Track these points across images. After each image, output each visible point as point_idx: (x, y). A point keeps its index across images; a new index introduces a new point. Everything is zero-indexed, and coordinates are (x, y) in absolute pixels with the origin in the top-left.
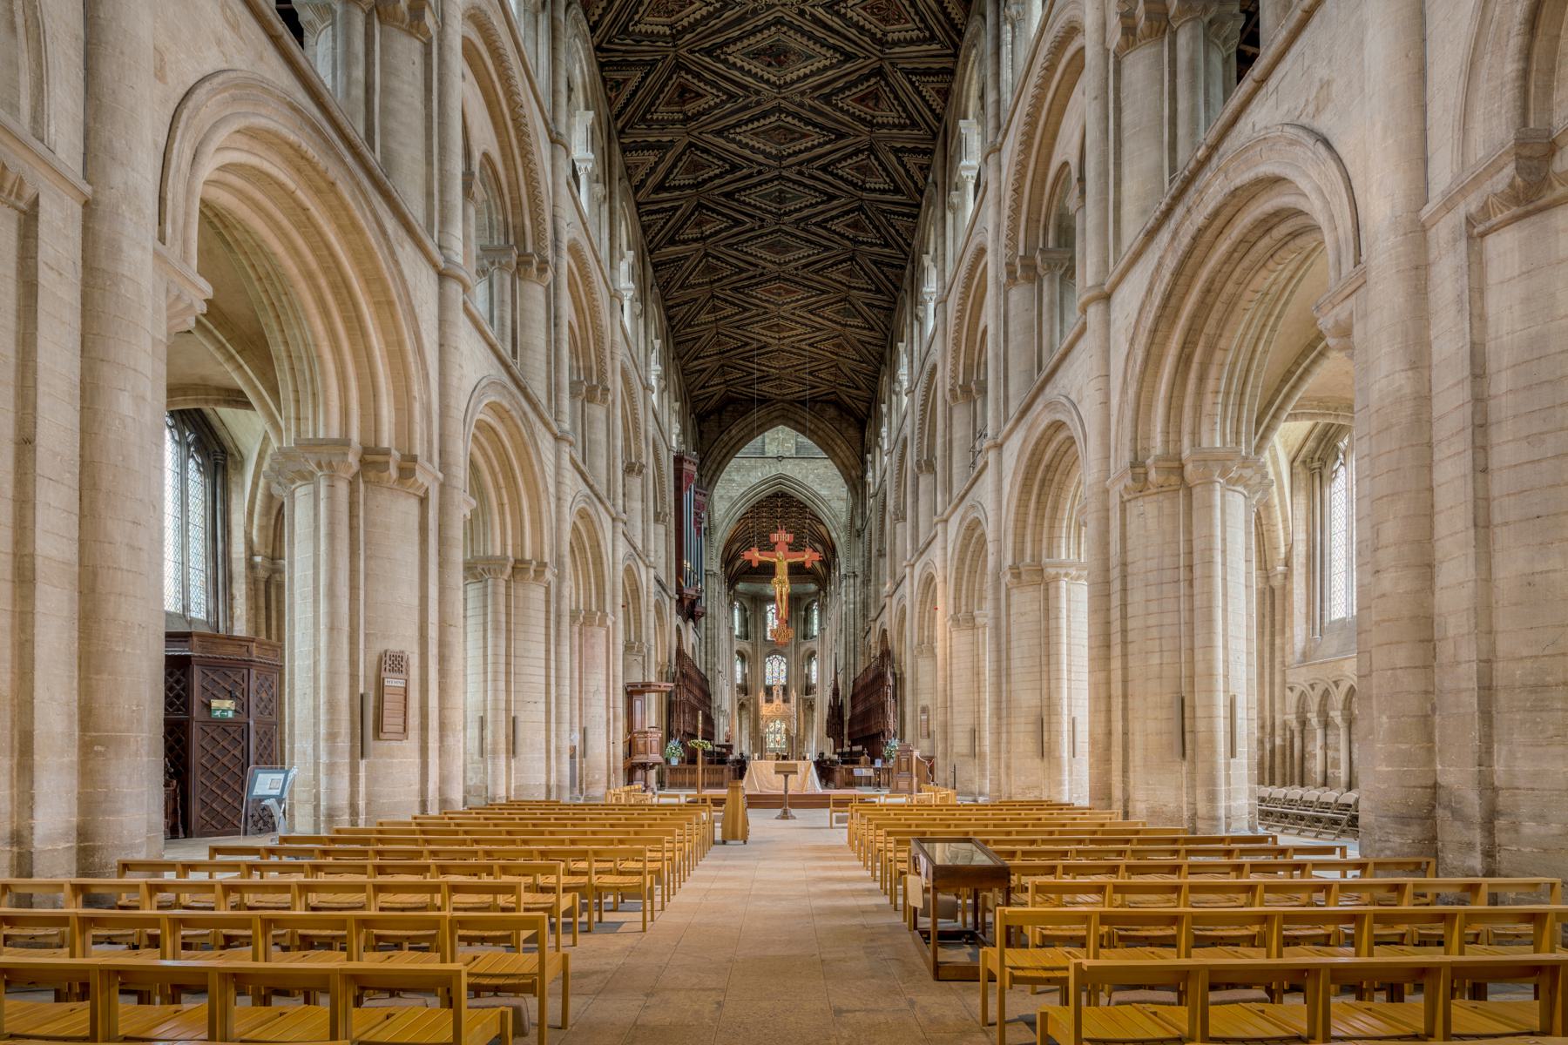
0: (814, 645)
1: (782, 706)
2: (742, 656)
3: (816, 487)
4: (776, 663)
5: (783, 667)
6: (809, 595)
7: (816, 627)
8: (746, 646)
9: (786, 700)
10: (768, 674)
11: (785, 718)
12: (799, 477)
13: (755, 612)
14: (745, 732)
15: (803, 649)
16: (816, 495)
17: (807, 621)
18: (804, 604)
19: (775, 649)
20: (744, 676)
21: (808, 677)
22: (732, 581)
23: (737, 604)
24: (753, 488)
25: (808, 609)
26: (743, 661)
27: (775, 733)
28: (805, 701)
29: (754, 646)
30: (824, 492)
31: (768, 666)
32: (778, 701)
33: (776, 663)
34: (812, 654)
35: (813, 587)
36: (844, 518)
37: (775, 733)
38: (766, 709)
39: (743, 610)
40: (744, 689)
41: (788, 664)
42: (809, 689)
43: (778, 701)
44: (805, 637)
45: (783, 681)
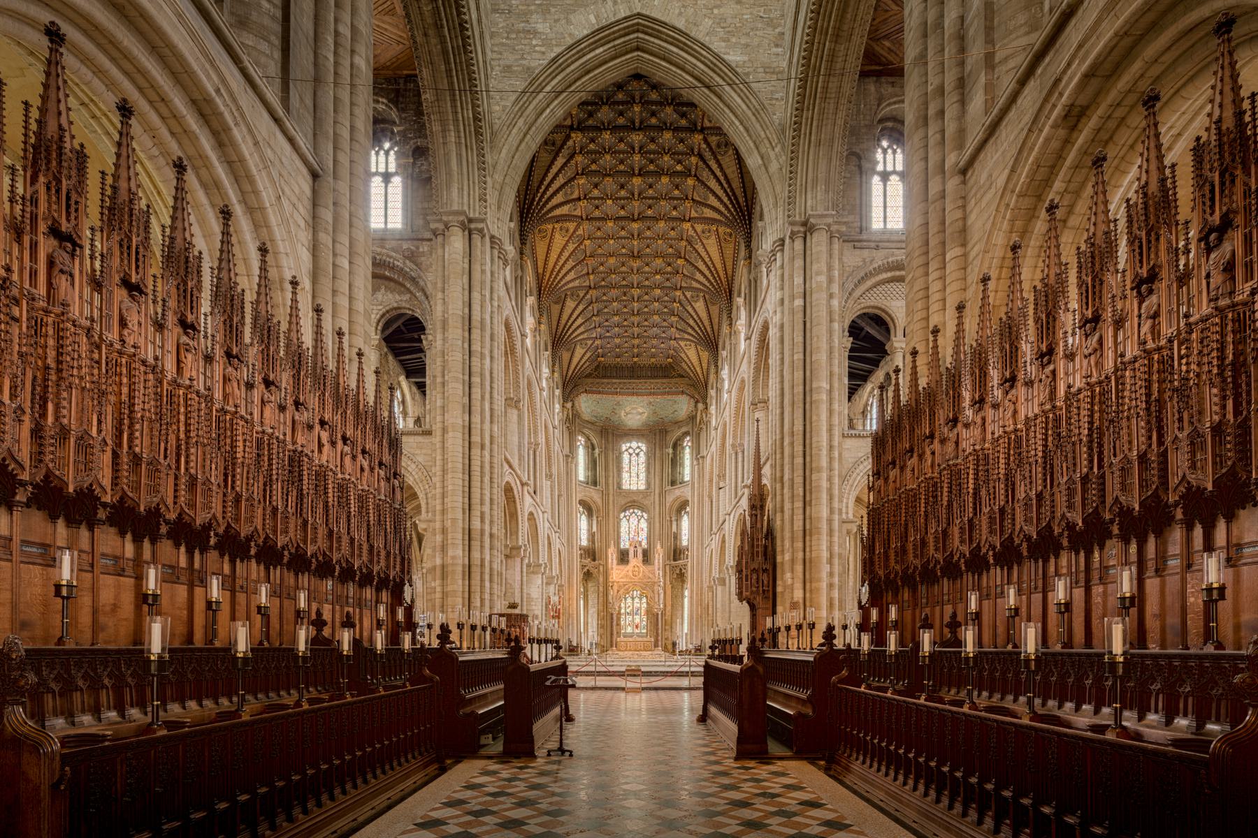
1: (642, 568)
3: (717, 46)
4: (634, 520)
5: (644, 525)
6: (677, 423)
7: (687, 471)
9: (647, 557)
10: (624, 535)
11: (647, 587)
12: (681, 24)
13: (605, 451)
14: (593, 611)
15: (670, 499)
16: (718, 63)
17: (675, 462)
18: (671, 439)
19: (633, 502)
22: (571, 386)
23: (581, 440)
24: (577, 48)
27: (632, 614)
29: (605, 495)
30: (733, 57)
31: (624, 523)
32: (635, 561)
33: (634, 520)
35: (682, 406)
37: (632, 614)
38: (618, 573)
39: (591, 447)
41: (649, 522)
43: (635, 561)
44: (673, 483)
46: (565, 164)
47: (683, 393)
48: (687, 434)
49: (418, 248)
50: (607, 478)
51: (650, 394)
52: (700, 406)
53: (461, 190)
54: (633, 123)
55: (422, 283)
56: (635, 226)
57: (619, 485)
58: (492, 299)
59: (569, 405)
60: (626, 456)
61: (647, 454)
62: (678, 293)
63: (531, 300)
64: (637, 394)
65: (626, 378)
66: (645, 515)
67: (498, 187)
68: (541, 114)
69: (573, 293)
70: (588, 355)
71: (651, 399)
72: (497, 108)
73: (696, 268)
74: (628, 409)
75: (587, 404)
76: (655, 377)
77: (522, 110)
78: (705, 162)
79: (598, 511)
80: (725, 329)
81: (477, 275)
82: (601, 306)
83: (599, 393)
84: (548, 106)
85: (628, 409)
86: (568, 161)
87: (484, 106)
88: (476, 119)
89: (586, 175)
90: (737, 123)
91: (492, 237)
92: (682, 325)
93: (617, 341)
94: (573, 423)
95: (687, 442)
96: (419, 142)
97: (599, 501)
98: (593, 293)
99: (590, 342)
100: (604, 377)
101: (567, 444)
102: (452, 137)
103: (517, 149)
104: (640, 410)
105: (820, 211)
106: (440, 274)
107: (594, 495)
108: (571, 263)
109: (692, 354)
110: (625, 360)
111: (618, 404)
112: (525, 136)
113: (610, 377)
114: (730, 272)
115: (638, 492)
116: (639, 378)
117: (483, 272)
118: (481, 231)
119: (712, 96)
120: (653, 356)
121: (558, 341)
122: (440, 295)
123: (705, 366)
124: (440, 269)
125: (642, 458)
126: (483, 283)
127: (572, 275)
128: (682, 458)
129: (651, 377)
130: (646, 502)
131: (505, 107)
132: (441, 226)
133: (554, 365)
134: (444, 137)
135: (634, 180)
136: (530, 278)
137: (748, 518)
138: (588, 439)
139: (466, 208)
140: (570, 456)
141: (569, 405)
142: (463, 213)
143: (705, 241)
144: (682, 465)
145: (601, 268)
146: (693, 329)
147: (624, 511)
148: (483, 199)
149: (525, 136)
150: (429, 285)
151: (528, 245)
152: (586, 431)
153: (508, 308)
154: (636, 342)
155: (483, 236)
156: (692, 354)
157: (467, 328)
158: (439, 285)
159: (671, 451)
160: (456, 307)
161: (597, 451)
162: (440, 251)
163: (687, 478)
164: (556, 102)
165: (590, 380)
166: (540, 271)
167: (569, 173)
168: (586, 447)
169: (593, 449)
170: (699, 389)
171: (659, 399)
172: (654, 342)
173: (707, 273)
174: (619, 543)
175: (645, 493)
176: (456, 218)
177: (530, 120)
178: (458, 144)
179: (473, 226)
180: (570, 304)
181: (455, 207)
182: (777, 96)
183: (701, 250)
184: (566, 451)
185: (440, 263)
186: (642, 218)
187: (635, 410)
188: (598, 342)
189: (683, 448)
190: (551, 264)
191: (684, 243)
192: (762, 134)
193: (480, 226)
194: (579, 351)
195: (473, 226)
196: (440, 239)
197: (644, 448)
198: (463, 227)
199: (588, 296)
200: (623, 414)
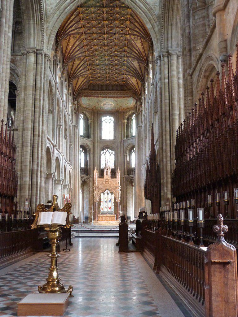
0: (134, 142)
2: (84, 148)
4: (108, 154)
5: (113, 157)
6: (129, 109)
8: (87, 142)
15: (125, 144)
17: (128, 126)
19: (107, 145)
20: (86, 163)
21: (129, 163)
22: (76, 94)
23: (82, 116)
25: (129, 119)
26: (85, 153)
28: (127, 179)
29: (93, 143)
31: (103, 157)
34: (132, 148)
35: (131, 102)
36: (157, 11)
39: (86, 119)
40: (86, 171)
41: (116, 155)
42: (131, 171)
45: (112, 166)
46: (75, 17)
47: (130, 97)
48: (133, 113)
49: (15, 58)
50: (95, 134)
51: (115, 97)
52: (138, 103)
53: (34, 39)
54: (103, 5)
55: (16, 71)
56: (105, 36)
57: (101, 137)
58: (44, 77)
59: (76, 102)
60: (104, 124)
61: (115, 122)
62: (126, 58)
63: (60, 65)
64: (109, 97)
65: (104, 90)
66: (114, 152)
67: (48, 35)
68: (66, 8)
69: (78, 58)
70: (85, 81)
71: (115, 99)
72: (49, 8)
73: (132, 50)
74: (104, 103)
75: (85, 101)
76: (117, 90)
77: (58, 8)
78: (133, 17)
79: (90, 150)
80: (146, 77)
81: (39, 70)
82: (91, 62)
83: (90, 96)
84: (69, 6)
85: (104, 103)
86: (77, 16)
87: (44, 10)
88: (41, 15)
89: (84, 20)
90: (142, 13)
91: (45, 54)
92: (128, 70)
93: (99, 75)
94: (77, 110)
95: (134, 117)
96: (18, 19)
97: (90, 146)
98: (88, 58)
99: (86, 76)
100: (93, 90)
101: (74, 120)
102: (32, 22)
103: (56, 21)
104: (111, 103)
105: (174, 48)
106: (24, 69)
107: (87, 142)
108: (78, 48)
109: (133, 81)
110: (103, 82)
111: (100, 101)
112: (59, 16)
113: (95, 90)
114: (147, 53)
115: (110, 141)
116: (109, 90)
117: (41, 68)
118: (41, 54)
119: (132, 3)
120: (116, 81)
121: (71, 77)
122: (24, 77)
123: (140, 85)
124: (24, 67)
125: (112, 124)
126: (41, 72)
127: (78, 52)
128: (131, 125)
129: (114, 90)
130: (114, 146)
131: (52, 8)
132: (25, 52)
133: (69, 87)
134: (29, 21)
135: (104, 22)
136: (59, 57)
137: (149, 164)
138: (85, 115)
139: (36, 46)
140: (76, 126)
141: (76, 102)
142: (35, 48)
143: (135, 42)
144: (131, 128)
145: (91, 49)
146: (133, 72)
147: (103, 150)
148: (42, 41)
149: (59, 16)
150: (19, 72)
151: (59, 47)
152: (84, 112)
153: (49, 74)
154: (108, 75)
155: (42, 55)
156: (133, 81)
157: (34, 90)
158: (24, 73)
159: (126, 121)
160: (31, 82)
161: (90, 121)
162: (25, 61)
163: (134, 134)
164: (72, 4)
165: (86, 91)
166: (64, 52)
167: (77, 19)
168: (84, 119)
169: (88, 120)
170: (138, 95)
171: (119, 99)
172: (116, 75)
173: (136, 52)
174: (100, 166)
175: (114, 141)
176: (32, 50)
177: (61, 11)
178: (34, 24)
179: (38, 52)
180: (77, 62)
181: (32, 46)
182: (157, 5)
183: (134, 44)
184: (74, 124)
185: (25, 65)
186: (108, 33)
187: (108, 103)
188: (90, 76)
189: (132, 120)
190: (69, 49)
191: (126, 42)
192: (152, 17)
193: (40, 52)
194: (81, 79)
195: (38, 52)
196: (25, 56)
197: (112, 119)
198: (34, 52)
199: (85, 59)
200: (102, 104)
